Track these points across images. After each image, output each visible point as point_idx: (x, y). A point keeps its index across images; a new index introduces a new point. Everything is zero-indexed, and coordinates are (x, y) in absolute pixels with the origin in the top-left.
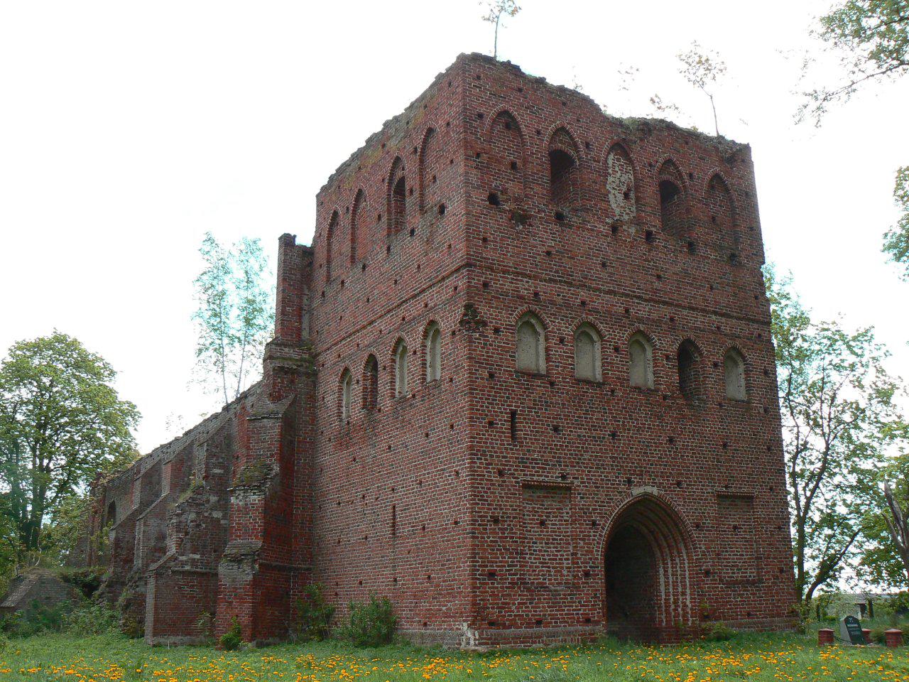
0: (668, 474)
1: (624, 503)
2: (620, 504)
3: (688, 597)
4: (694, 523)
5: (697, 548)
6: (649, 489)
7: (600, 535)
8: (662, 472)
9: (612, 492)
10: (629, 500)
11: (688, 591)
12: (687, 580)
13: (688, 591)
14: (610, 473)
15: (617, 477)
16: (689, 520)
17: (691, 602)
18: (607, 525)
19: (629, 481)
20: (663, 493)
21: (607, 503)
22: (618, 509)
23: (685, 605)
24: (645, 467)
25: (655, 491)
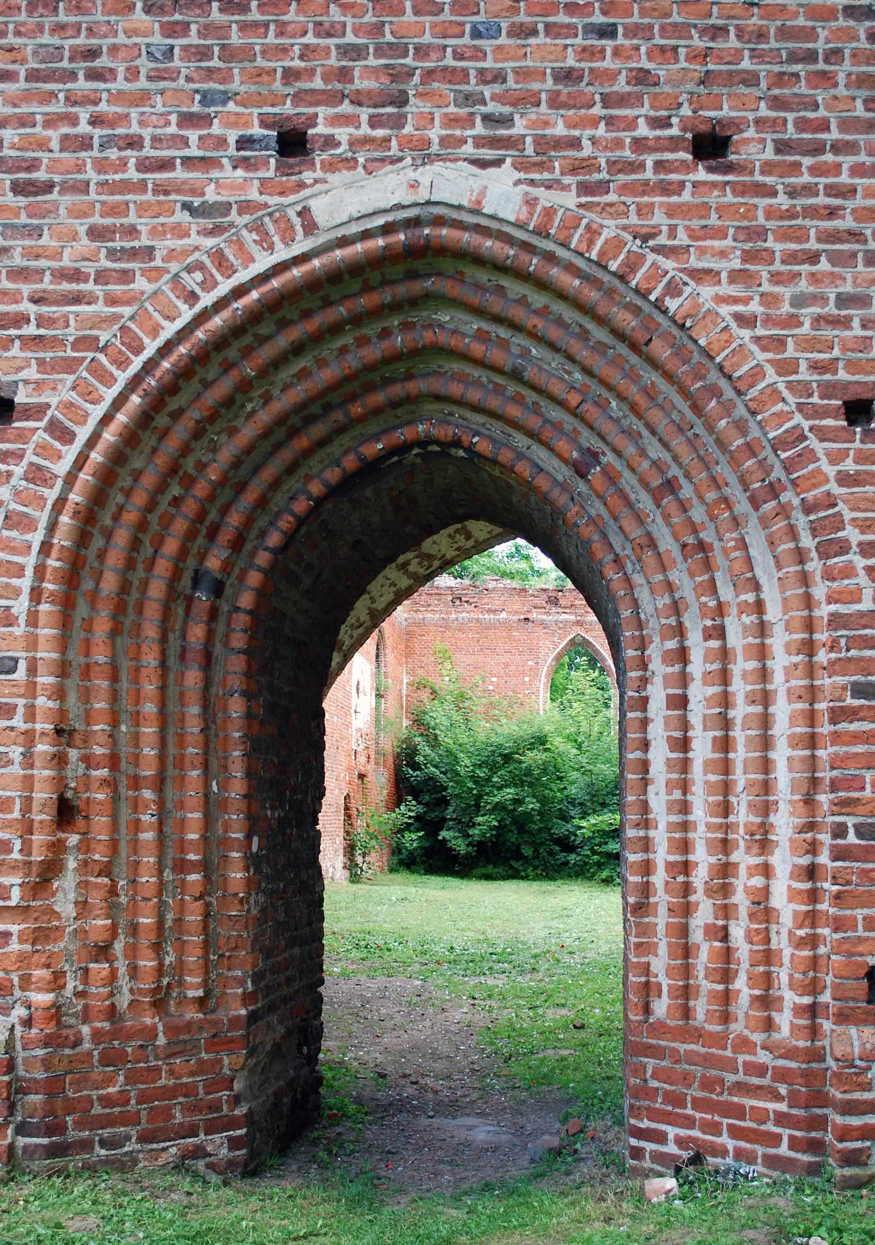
0: (622, 85)
1: (243, 276)
2: (209, 284)
3: (784, 861)
4: (828, 390)
5: (843, 548)
6: (451, 184)
7: (37, 475)
8: (567, 76)
9: (143, 209)
10: (282, 254)
11: (785, 823)
12: (782, 754)
13: (785, 823)
14: (143, 98)
15: (189, 120)
16: (786, 367)
17: (793, 895)
18: (97, 412)
19: (293, 144)
20: (570, 200)
21: (101, 277)
22: (187, 314)
23: (763, 910)
24: (421, 52)
25: (502, 194)
